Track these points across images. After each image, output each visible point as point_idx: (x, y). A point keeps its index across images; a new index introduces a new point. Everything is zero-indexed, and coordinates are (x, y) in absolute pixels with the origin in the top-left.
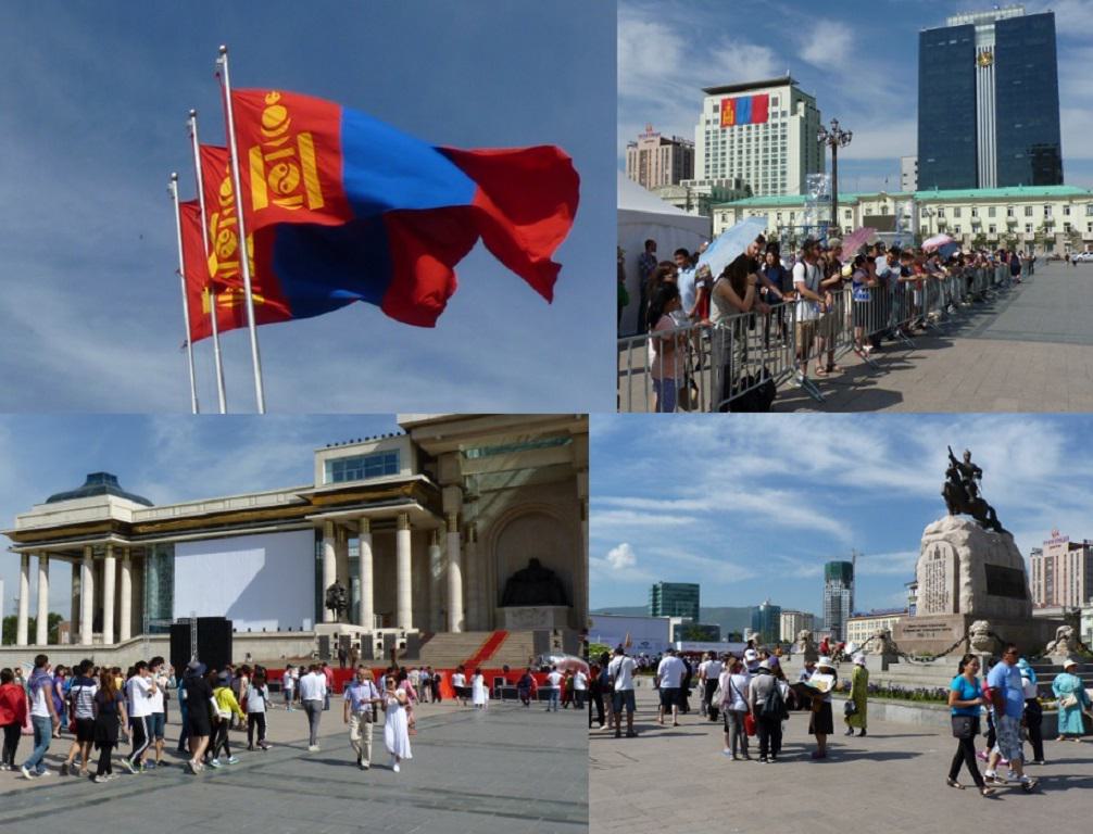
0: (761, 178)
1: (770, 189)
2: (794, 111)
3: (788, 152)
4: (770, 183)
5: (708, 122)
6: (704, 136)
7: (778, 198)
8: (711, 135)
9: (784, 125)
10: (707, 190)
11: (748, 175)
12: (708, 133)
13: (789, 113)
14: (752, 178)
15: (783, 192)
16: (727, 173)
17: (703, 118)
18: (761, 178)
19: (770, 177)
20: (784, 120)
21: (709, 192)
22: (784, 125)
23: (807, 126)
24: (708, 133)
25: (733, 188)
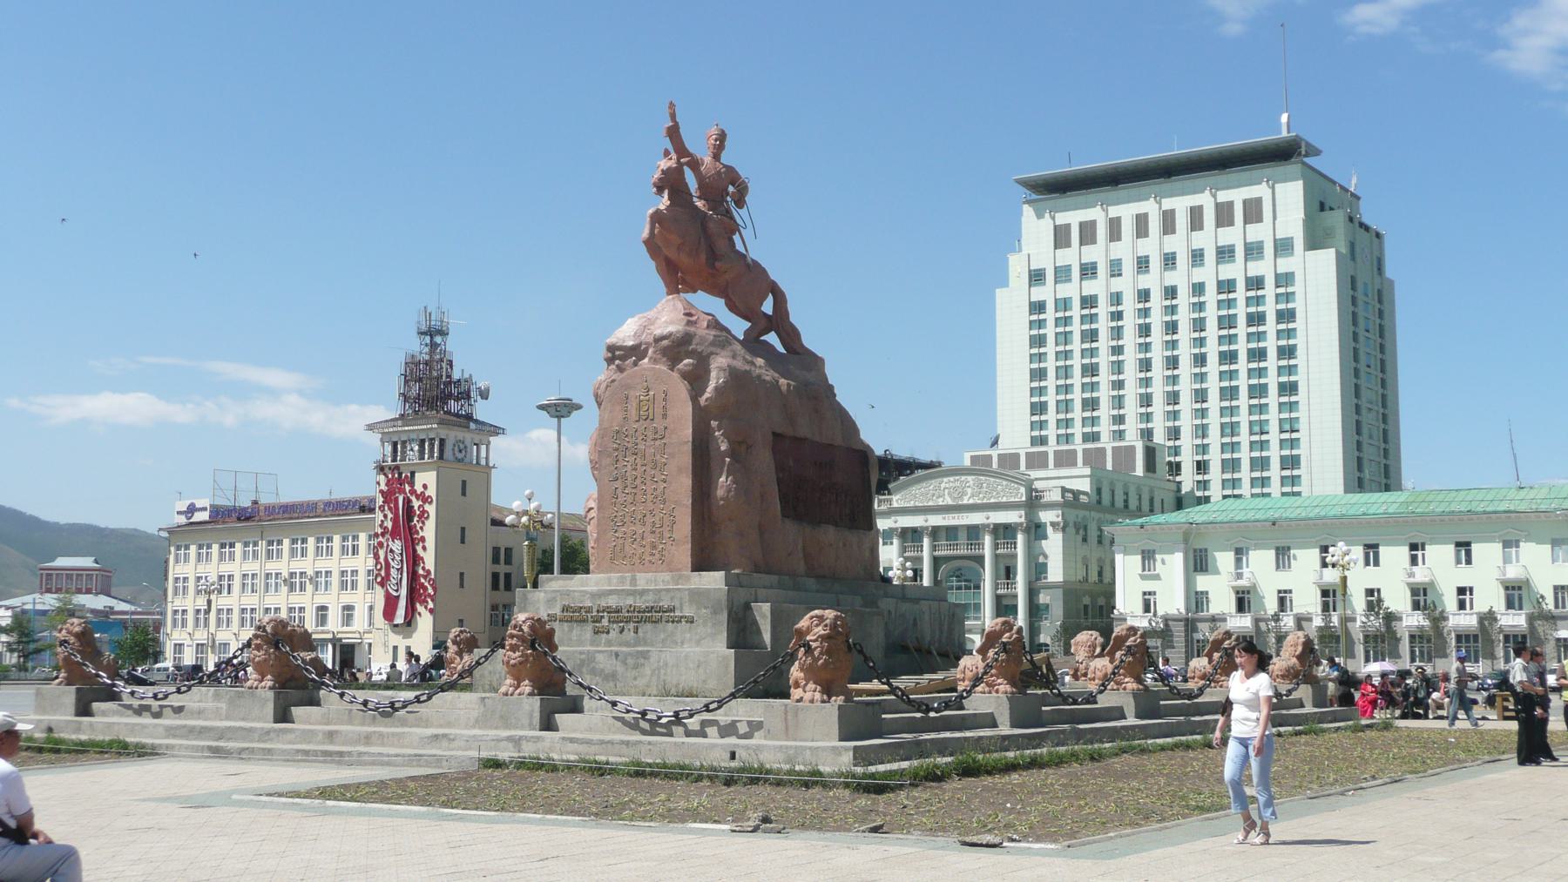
0: (1214, 439)
1: (1245, 474)
2: (1315, 241)
3: (1300, 360)
4: (1244, 455)
5: (1036, 277)
6: (1024, 317)
7: (1276, 504)
8: (1050, 315)
9: (1284, 279)
10: (1080, 480)
11: (1175, 433)
12: (1038, 307)
13: (1299, 244)
14: (1187, 442)
15: (1294, 480)
16: (1105, 428)
17: (1017, 267)
18: (1214, 439)
19: (1244, 438)
20: (1285, 265)
21: (1084, 485)
22: (1284, 279)
23: (1353, 280)
24: (1038, 307)
25: (1139, 470)
